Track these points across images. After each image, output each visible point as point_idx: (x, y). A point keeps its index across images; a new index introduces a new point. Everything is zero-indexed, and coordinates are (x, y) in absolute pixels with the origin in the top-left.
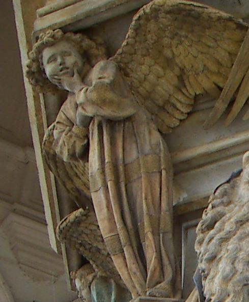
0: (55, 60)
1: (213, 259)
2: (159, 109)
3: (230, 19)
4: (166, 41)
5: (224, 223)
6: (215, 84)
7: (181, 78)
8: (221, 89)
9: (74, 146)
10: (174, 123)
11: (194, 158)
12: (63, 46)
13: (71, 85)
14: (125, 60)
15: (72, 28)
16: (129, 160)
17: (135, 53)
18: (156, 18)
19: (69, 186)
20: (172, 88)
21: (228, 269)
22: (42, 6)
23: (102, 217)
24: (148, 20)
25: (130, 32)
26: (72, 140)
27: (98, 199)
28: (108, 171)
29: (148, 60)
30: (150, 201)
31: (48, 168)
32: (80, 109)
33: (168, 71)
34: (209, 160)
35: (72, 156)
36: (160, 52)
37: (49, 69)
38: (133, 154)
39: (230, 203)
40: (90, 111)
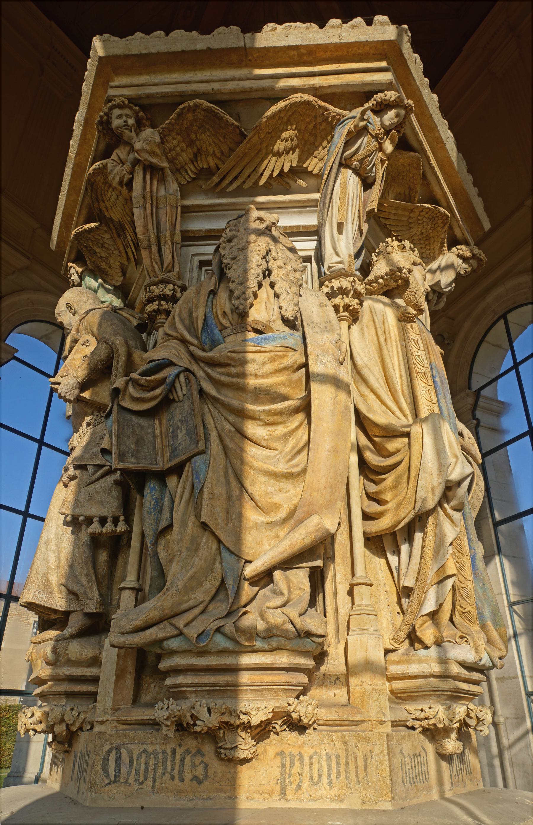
3: (238, 127)
4: (195, 128)
6: (216, 164)
7: (196, 155)
8: (218, 169)
10: (184, 182)
12: (127, 111)
17: (173, 131)
19: (96, 206)
23: (139, 224)
24: (189, 110)
29: (179, 138)
33: (189, 148)
34: (201, 210)
35: (121, 183)
36: (188, 135)
37: (116, 123)
38: (162, 192)
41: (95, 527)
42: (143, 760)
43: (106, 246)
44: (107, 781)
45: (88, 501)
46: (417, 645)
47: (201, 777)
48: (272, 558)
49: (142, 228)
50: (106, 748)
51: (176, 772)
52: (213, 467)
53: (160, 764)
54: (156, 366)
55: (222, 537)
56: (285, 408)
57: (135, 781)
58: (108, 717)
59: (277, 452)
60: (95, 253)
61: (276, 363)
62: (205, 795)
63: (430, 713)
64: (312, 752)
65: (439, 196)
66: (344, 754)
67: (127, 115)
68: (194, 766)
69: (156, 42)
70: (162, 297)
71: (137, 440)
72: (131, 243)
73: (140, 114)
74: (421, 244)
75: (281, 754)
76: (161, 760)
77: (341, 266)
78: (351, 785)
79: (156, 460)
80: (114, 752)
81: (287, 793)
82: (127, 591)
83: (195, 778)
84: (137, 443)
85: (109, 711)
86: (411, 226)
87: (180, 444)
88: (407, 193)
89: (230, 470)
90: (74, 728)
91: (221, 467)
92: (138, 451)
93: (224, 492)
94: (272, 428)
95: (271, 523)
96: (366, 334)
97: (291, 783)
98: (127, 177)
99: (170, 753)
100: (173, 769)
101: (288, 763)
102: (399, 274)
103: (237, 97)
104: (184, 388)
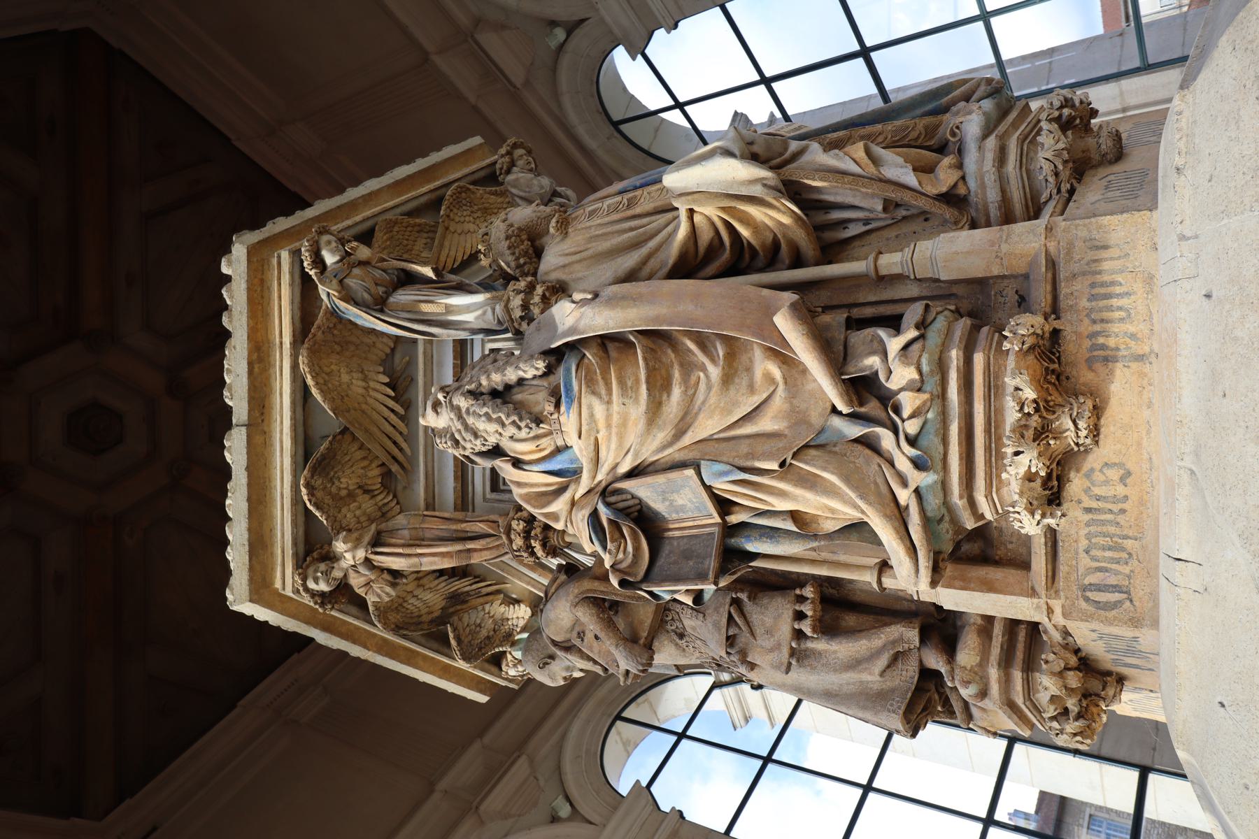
3: (334, 437)
4: (334, 490)
7: (366, 492)
8: (383, 464)
11: (426, 499)
12: (310, 571)
29: (344, 510)
35: (393, 585)
36: (341, 498)
37: (323, 587)
41: (806, 627)
42: (1099, 553)
43: (478, 621)
44: (1128, 603)
45: (772, 636)
46: (962, 190)
47: (1122, 472)
50: (1083, 605)
51: (1115, 508)
53: (1104, 529)
57: (1127, 563)
58: (1042, 601)
60: (488, 638)
62: (1145, 466)
63: (1047, 168)
64: (1086, 321)
66: (1089, 277)
68: (1106, 482)
69: (237, 533)
70: (527, 535)
72: (474, 586)
75: (1090, 362)
76: (1099, 529)
78: (1130, 265)
80: (1089, 594)
81: (1141, 353)
82: (883, 579)
83: (1123, 480)
85: (1035, 601)
87: (690, 501)
90: (1073, 661)
92: (698, 557)
96: (580, 275)
97: (1128, 348)
98: (386, 576)
99: (1090, 516)
100: (1111, 511)
101: (1101, 353)
103: (301, 438)
104: (624, 497)
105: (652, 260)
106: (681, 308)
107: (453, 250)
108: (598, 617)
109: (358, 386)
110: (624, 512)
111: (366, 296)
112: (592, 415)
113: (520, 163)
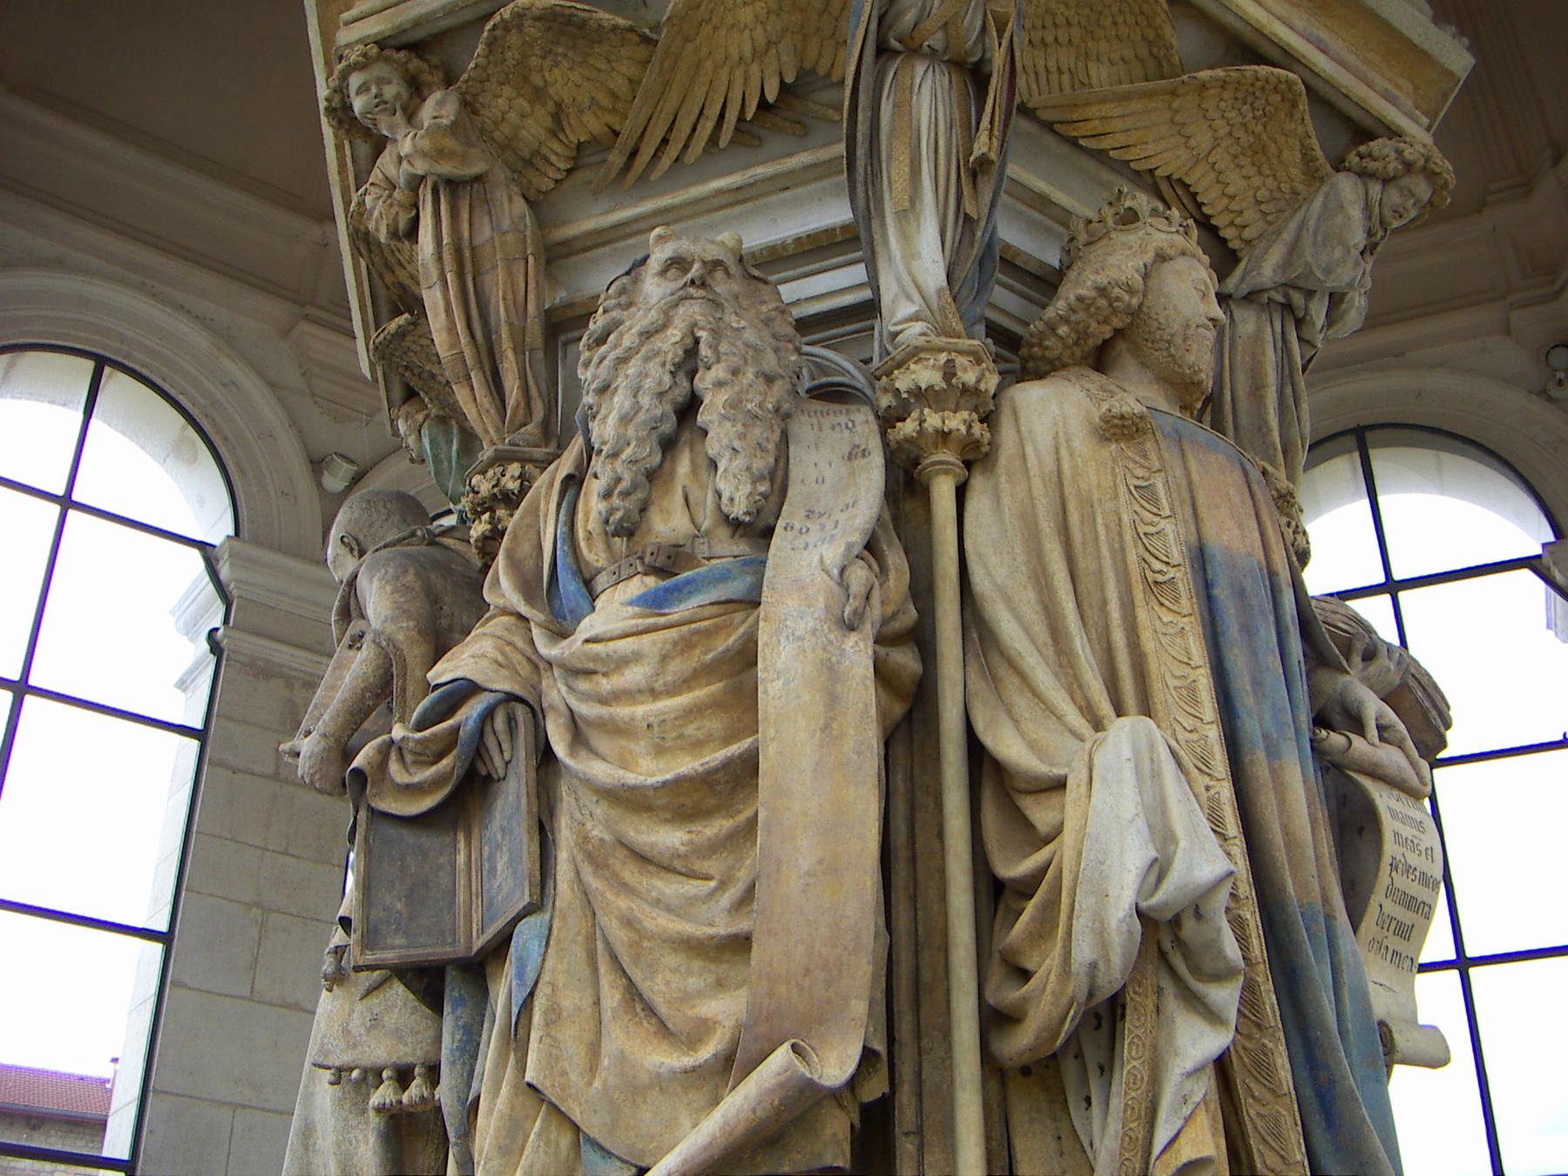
0: (368, 90)
1: (605, 389)
2: (524, 164)
3: (631, 29)
4: (534, 61)
5: (621, 335)
7: (557, 117)
8: (617, 134)
9: (395, 219)
11: (576, 238)
13: (392, 128)
14: (473, 91)
15: (392, 43)
16: (478, 241)
18: (520, 27)
19: (389, 279)
20: (542, 132)
21: (628, 404)
22: (349, 8)
24: (507, 30)
25: (480, 49)
26: (393, 211)
27: (433, 299)
28: (447, 256)
29: (507, 91)
30: (510, 302)
31: (356, 252)
32: (405, 163)
33: (538, 107)
35: (394, 234)
36: (526, 79)
37: (358, 104)
38: (485, 232)
39: (630, 305)
40: (420, 167)
41: (383, 1094)
48: (686, 1161)
49: (444, 335)
52: (559, 941)
54: (442, 698)
55: (577, 1116)
56: (716, 770)
59: (712, 884)
60: (433, 376)
61: (697, 651)
65: (1249, 35)
67: (381, 82)
71: (412, 890)
73: (410, 66)
74: (1240, 167)
77: (918, 327)
79: (454, 932)
84: (410, 896)
86: (1187, 132)
88: (1144, 53)
89: (600, 945)
91: (580, 938)
93: (587, 1002)
94: (697, 827)
95: (694, 1069)
96: (1006, 500)
102: (1103, 303)
104: (505, 746)
105: (1017, 681)
106: (804, 842)
107: (1129, 122)
108: (364, 690)
109: (740, 44)
110: (478, 750)
111: (909, 17)
112: (623, 662)
113: (1394, 196)
